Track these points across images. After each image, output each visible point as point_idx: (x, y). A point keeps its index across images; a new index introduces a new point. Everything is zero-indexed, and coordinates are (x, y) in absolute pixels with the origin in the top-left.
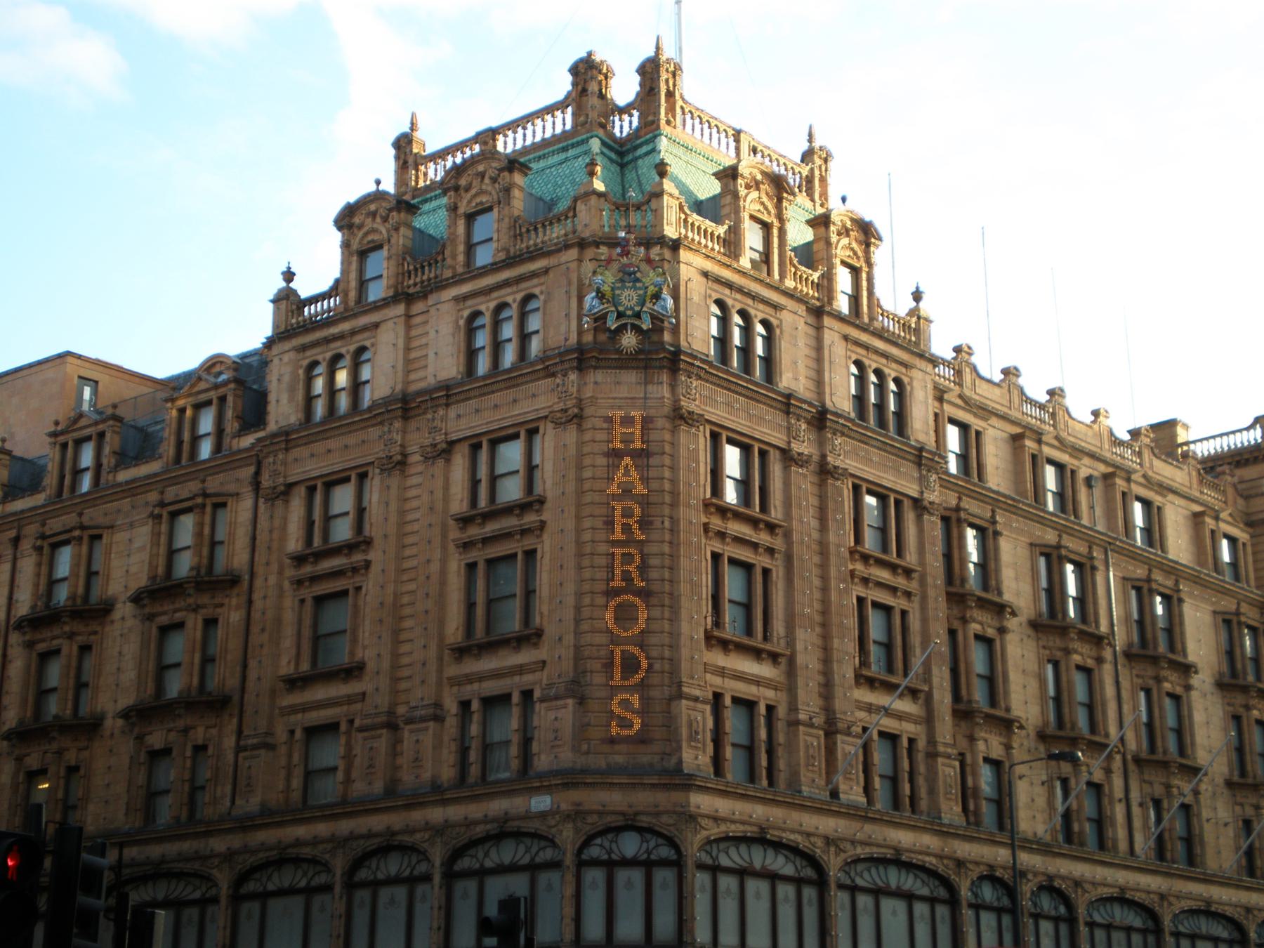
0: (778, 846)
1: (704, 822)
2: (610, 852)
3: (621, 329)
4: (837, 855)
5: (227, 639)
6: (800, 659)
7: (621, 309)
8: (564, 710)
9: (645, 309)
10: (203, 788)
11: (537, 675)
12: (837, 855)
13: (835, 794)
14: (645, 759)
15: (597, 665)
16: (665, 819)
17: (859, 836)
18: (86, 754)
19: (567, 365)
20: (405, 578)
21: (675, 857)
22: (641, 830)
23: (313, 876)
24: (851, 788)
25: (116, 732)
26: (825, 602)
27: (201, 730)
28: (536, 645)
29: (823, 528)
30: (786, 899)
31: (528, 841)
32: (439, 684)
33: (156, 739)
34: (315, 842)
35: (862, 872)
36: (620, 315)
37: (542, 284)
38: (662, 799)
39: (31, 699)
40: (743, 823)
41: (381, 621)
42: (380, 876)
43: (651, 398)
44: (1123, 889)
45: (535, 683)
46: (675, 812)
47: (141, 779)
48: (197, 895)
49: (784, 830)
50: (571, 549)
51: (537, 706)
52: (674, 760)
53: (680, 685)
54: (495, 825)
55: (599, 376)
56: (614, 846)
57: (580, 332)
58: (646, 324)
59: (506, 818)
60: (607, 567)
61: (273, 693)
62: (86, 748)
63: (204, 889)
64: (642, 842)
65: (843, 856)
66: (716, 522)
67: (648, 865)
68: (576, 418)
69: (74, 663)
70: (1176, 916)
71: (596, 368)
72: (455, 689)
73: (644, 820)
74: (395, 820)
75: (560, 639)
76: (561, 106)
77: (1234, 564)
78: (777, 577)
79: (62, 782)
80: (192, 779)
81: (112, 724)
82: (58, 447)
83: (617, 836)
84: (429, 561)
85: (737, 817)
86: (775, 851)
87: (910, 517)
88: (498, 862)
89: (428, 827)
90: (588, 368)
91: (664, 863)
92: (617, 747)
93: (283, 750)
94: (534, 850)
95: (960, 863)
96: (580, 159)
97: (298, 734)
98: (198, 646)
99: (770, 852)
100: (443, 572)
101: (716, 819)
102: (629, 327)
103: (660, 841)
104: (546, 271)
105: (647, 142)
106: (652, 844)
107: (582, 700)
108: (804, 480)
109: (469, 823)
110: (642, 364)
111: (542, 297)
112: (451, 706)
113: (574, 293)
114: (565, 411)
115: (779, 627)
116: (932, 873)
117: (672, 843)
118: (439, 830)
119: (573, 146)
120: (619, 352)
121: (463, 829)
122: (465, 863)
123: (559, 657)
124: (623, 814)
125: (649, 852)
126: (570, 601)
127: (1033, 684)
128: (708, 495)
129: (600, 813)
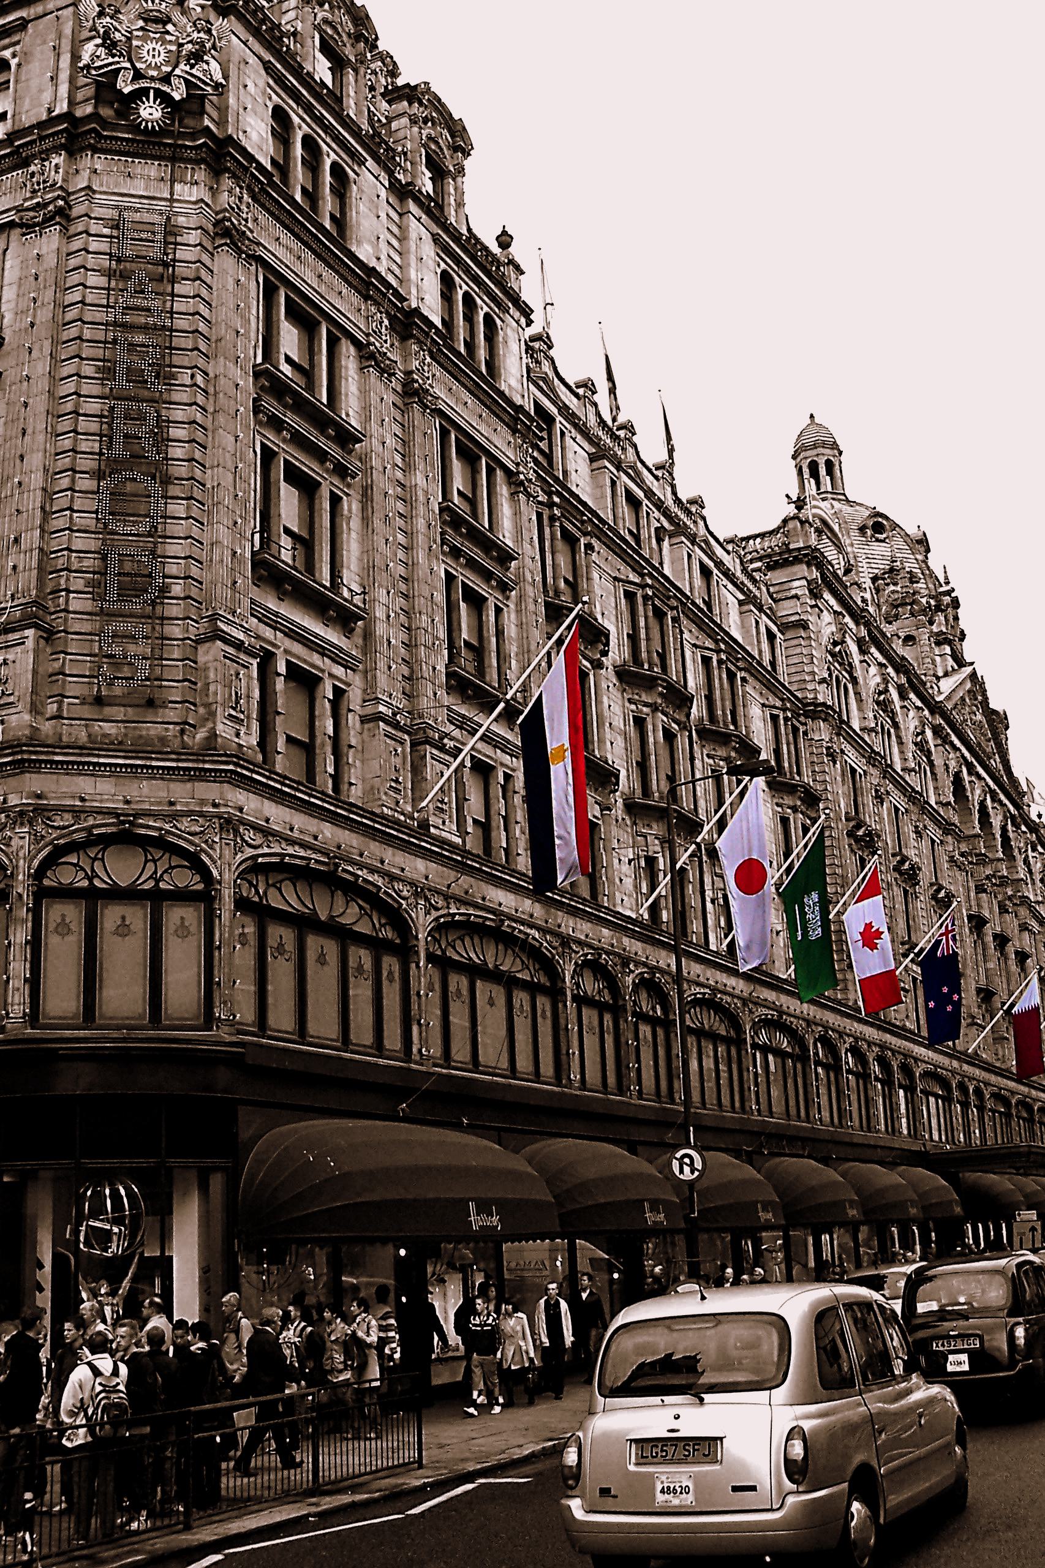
0: (354, 890)
1: (249, 835)
4: (427, 913)
6: (380, 629)
7: (138, 65)
8: (19, 649)
9: (177, 72)
12: (427, 913)
13: (424, 825)
14: (155, 730)
17: (455, 889)
19: (48, 144)
22: (145, 843)
24: (444, 823)
26: (410, 565)
29: (408, 468)
30: (360, 968)
35: (454, 941)
36: (138, 75)
37: (18, 43)
38: (182, 793)
40: (304, 845)
44: (714, 990)
46: (201, 814)
49: (361, 866)
50: (40, 404)
52: (201, 735)
53: (214, 618)
55: (99, 162)
56: (97, 865)
57: (72, 103)
60: (101, 435)
64: (146, 861)
65: (435, 914)
66: (271, 405)
70: (754, 1023)
71: (95, 150)
73: (150, 827)
75: (17, 540)
77: (773, 663)
78: (350, 510)
83: (104, 850)
85: (296, 834)
86: (345, 894)
87: (503, 490)
90: (82, 149)
91: (182, 896)
92: (108, 711)
95: (566, 941)
99: (340, 899)
101: (267, 833)
102: (152, 92)
107: (48, 635)
108: (385, 394)
110: (168, 152)
113: (66, 46)
115: (351, 578)
116: (534, 953)
120: (135, 128)
123: (15, 567)
126: (37, 480)
127: (620, 742)
128: (259, 360)
129: (76, 812)
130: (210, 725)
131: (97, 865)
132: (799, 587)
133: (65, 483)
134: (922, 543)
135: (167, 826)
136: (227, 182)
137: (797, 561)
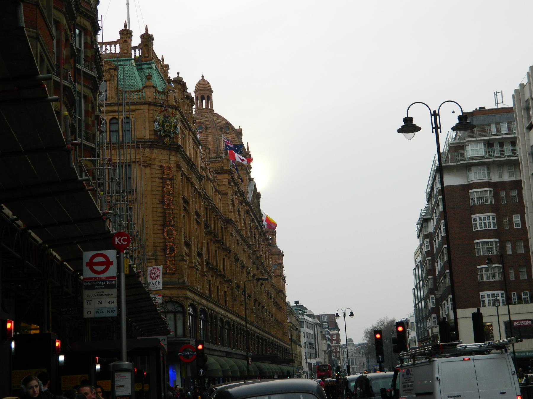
2: (165, 309)
3: (165, 136)
7: (165, 129)
14: (174, 280)
15: (159, 249)
16: (181, 299)
21: (182, 310)
38: (180, 293)
43: (171, 160)
46: (183, 297)
55: (155, 151)
58: (172, 135)
67: (175, 313)
68: (147, 164)
71: (155, 148)
76: (115, 43)
91: (179, 312)
96: (127, 66)
103: (178, 305)
104: (134, 111)
105: (147, 64)
106: (176, 306)
107: (155, 259)
111: (133, 120)
114: (145, 161)
117: (182, 306)
119: (123, 60)
124: (170, 297)
125: (175, 309)
130: (183, 278)
131: (166, 306)
132: (225, 182)
133: (156, 227)
134: (239, 133)
135: (178, 299)
136: (178, 155)
137: (226, 173)
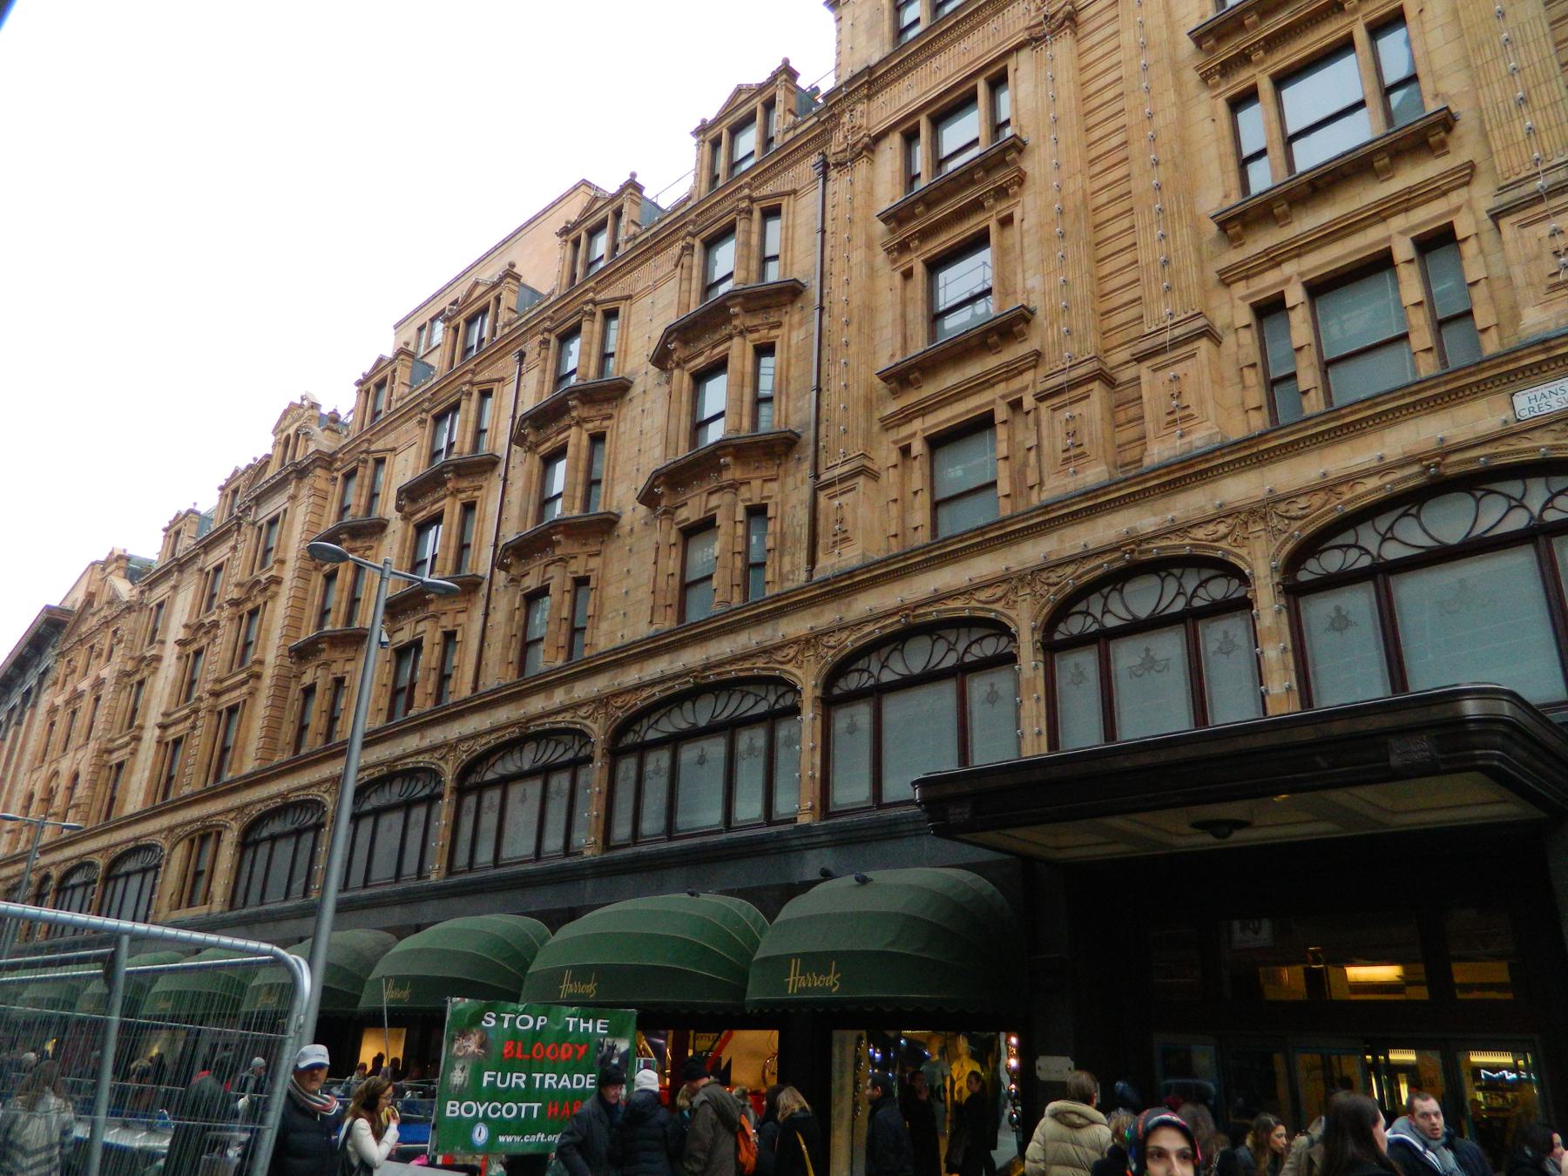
5: (789, 365)
10: (761, 565)
11: (1455, 198)
18: (594, 563)
20: (1098, 168)
23: (969, 646)
25: (637, 527)
27: (756, 484)
28: (1440, 149)
31: (1514, 488)
32: (1203, 285)
33: (691, 512)
34: (969, 591)
39: (531, 509)
41: (1062, 236)
42: (1111, 622)
45: (1458, 209)
47: (673, 565)
48: (762, 708)
51: (1469, 249)
54: (1416, 469)
59: (1446, 450)
61: (869, 404)
62: (598, 554)
63: (772, 698)
69: (584, 455)
72: (1240, 289)
74: (1144, 520)
79: (568, 597)
80: (746, 553)
81: (632, 513)
82: (569, 244)
84: (1150, 117)
88: (1429, 543)
89: (1226, 513)
93: (891, 478)
94: (1536, 500)
97: (918, 447)
98: (748, 380)
100: (1182, 123)
109: (1330, 486)
112: (1232, 310)
118: (1257, 512)
121: (1317, 500)
122: (1332, 561)
